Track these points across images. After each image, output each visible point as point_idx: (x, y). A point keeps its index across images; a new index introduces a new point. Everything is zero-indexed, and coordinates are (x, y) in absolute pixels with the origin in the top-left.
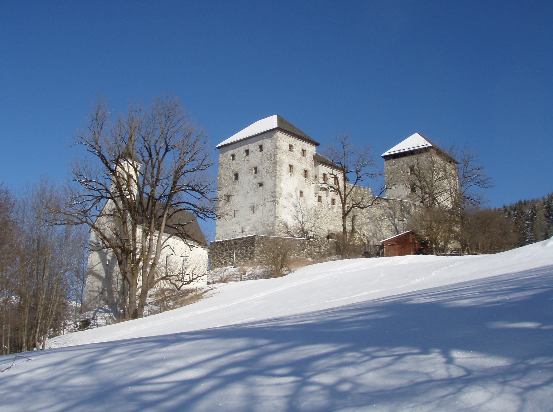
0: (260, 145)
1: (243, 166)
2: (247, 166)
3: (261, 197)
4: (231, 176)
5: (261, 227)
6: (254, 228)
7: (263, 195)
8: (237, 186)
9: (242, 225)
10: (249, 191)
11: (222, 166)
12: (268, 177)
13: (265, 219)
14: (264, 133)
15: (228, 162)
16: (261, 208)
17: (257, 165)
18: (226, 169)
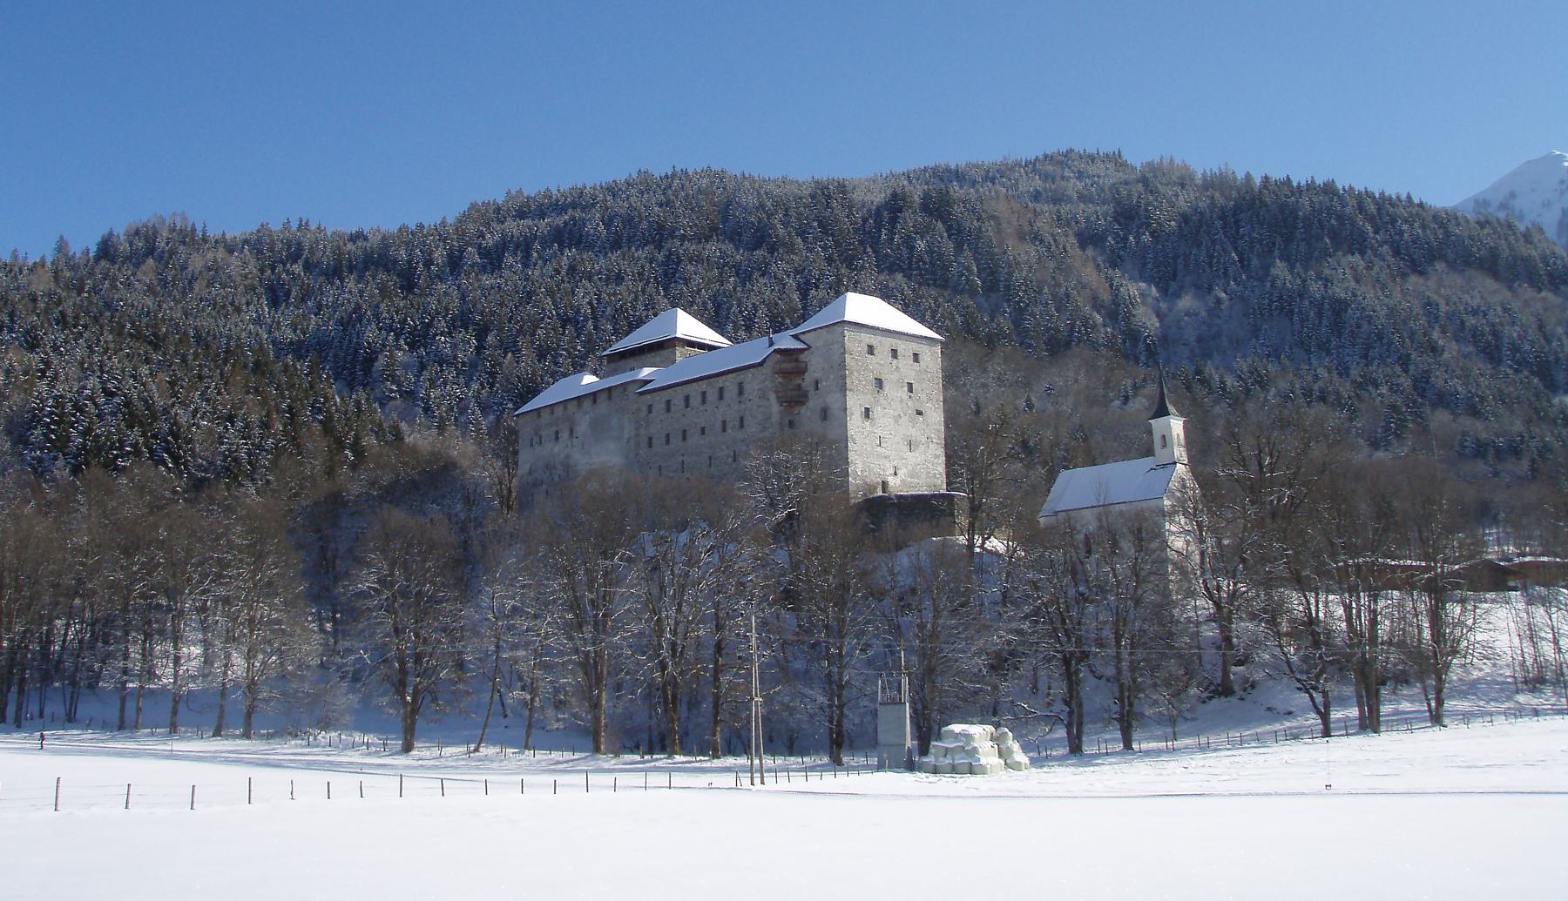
9: (895, 463)
10: (902, 415)
16: (922, 448)
17: (912, 382)
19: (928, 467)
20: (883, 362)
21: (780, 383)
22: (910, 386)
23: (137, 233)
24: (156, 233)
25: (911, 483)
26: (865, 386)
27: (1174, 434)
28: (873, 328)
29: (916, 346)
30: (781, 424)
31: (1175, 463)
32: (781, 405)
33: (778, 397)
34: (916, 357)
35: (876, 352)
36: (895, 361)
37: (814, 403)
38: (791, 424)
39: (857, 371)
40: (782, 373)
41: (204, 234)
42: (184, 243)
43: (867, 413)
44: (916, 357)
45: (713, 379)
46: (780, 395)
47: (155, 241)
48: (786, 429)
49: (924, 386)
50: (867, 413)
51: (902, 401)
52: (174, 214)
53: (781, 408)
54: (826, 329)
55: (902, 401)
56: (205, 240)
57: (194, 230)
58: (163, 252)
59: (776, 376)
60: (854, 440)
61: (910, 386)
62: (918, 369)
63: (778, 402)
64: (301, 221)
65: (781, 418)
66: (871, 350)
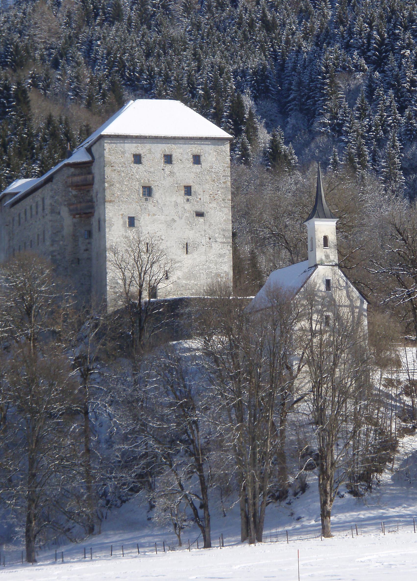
0: (195, 154)
1: (162, 178)
2: (170, 180)
3: (203, 233)
4: (137, 188)
5: (203, 276)
6: (190, 275)
7: (205, 231)
8: (150, 206)
10: (176, 218)
11: (114, 168)
12: (215, 206)
13: (212, 266)
14: (207, 139)
15: (126, 163)
16: (202, 249)
17: (191, 184)
18: (123, 175)
19: (209, 268)
21: (75, 196)
22: (188, 190)
25: (186, 284)
28: (137, 137)
29: (196, 149)
30: (74, 235)
31: (316, 266)
32: (74, 217)
33: (70, 210)
34: (197, 159)
35: (144, 160)
37: (96, 214)
39: (120, 183)
40: (76, 186)
43: (132, 222)
44: (197, 159)
45: (34, 194)
46: (72, 207)
49: (207, 186)
50: (132, 222)
51: (176, 204)
53: (75, 220)
55: (176, 204)
59: (70, 189)
61: (188, 190)
62: (198, 171)
63: (71, 215)
66: (138, 159)
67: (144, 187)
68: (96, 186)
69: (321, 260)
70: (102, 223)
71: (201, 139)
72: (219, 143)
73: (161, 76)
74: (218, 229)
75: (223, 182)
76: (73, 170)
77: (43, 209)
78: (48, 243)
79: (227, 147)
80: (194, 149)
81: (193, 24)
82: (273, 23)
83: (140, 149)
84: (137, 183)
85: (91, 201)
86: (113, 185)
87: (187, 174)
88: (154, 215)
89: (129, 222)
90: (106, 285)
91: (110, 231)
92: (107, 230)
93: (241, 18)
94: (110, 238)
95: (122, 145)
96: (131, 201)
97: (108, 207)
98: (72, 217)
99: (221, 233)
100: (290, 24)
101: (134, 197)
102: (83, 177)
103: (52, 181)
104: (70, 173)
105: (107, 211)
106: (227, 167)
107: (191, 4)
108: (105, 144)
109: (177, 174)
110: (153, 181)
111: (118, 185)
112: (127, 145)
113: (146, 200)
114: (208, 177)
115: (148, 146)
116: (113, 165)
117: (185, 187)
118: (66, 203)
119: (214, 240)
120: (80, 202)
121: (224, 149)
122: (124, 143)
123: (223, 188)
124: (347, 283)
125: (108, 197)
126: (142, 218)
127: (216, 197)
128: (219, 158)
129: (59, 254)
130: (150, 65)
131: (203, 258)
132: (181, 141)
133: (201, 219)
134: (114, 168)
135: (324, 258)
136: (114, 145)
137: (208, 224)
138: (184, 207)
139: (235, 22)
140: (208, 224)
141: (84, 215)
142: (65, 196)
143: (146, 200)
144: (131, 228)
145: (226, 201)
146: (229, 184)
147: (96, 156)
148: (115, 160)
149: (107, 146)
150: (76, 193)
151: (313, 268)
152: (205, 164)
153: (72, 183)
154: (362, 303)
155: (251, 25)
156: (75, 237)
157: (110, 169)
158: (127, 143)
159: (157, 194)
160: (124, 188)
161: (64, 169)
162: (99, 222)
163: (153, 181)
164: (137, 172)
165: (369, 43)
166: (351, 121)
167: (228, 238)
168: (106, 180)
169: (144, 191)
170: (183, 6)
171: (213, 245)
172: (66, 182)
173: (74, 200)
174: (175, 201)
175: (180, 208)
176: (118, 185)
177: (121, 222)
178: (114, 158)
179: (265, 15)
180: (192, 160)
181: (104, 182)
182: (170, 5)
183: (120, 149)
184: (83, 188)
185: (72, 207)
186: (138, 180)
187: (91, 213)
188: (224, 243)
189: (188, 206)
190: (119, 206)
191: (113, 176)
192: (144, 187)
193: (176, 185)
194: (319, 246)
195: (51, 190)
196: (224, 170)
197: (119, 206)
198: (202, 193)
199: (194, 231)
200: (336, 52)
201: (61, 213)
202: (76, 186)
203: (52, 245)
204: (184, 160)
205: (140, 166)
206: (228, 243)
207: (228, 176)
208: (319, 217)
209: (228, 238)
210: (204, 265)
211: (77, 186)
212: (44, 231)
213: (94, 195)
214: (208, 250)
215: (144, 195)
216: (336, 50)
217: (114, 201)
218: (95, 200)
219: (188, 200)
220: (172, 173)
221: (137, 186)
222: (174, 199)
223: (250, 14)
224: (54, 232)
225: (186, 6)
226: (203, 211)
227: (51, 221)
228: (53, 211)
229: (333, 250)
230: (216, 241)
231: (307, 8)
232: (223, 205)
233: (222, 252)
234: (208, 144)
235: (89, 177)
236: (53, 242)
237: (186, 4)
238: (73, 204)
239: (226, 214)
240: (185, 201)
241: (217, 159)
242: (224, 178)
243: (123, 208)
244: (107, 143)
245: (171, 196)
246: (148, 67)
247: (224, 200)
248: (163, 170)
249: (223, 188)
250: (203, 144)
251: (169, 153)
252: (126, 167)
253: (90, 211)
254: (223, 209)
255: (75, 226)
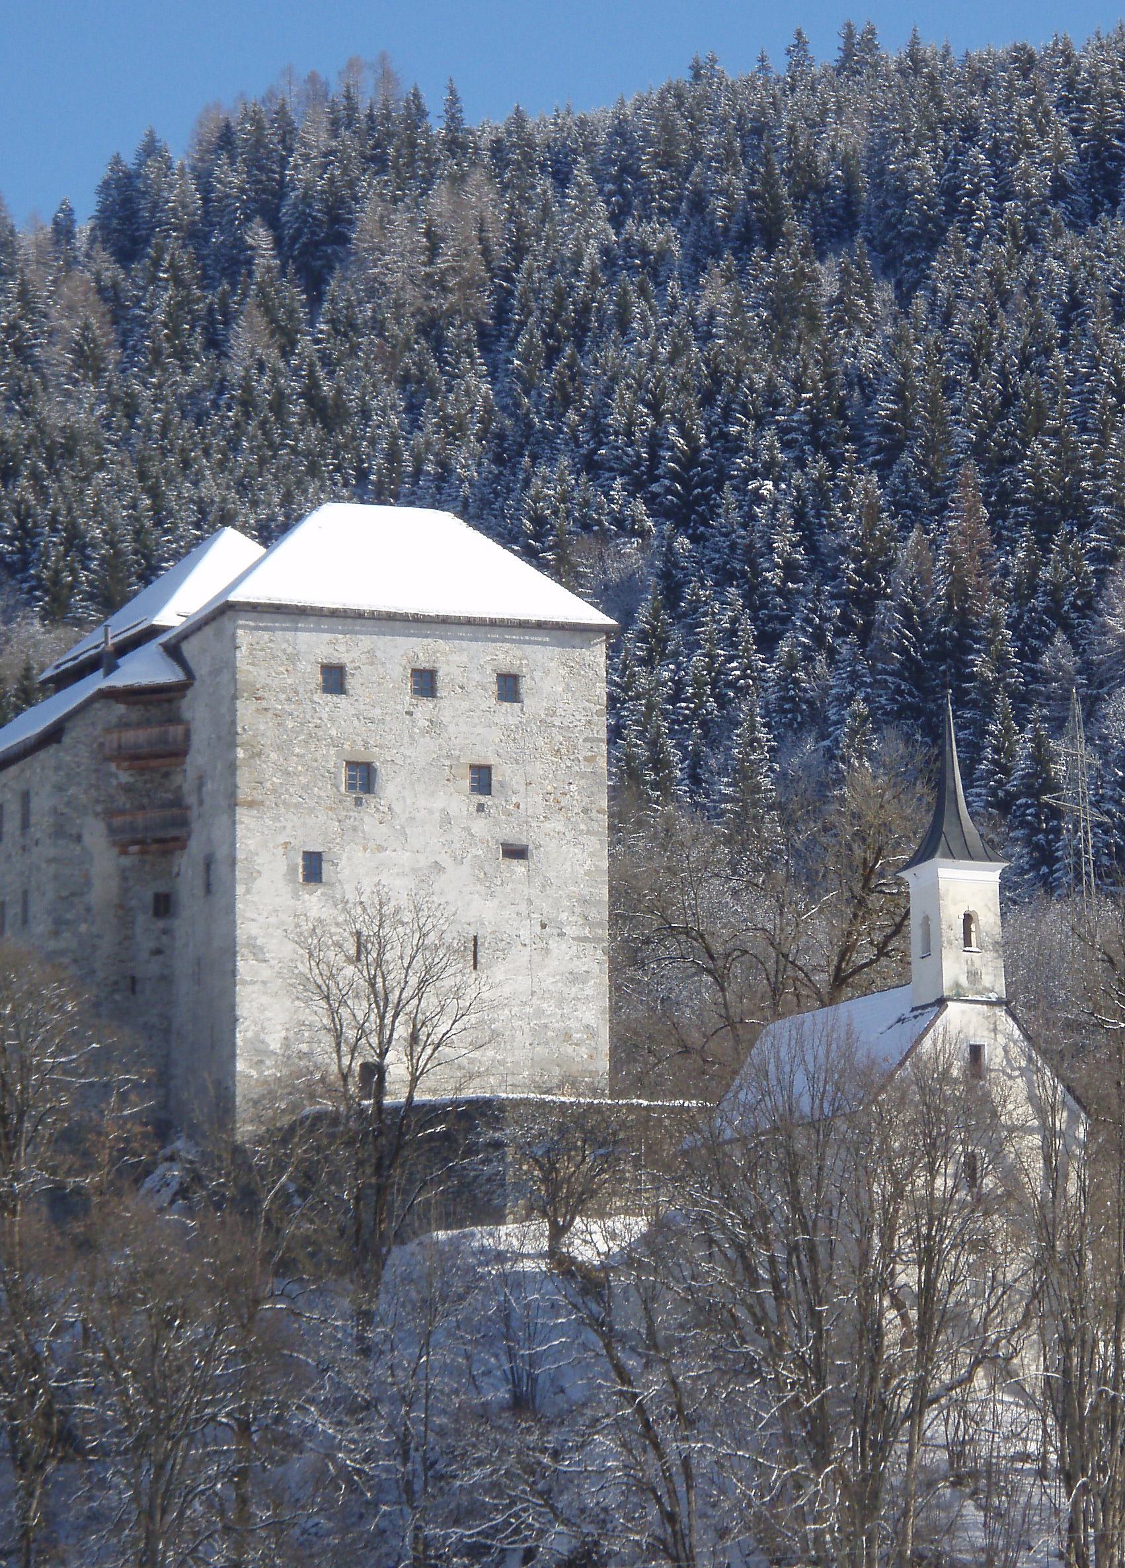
1: (406, 739)
3: (523, 907)
4: (331, 765)
5: (523, 1038)
7: (530, 902)
8: (368, 821)
10: (446, 861)
11: (264, 704)
12: (560, 827)
13: (549, 1007)
14: (540, 626)
15: (301, 690)
16: (520, 956)
17: (492, 760)
18: (290, 724)
19: (540, 1013)
20: (377, 712)
21: (128, 789)
22: (482, 779)
23: (226, 140)
24: (287, 132)
26: (306, 787)
27: (952, 915)
30: (121, 906)
31: (941, 1002)
32: (124, 852)
33: (112, 831)
35: (351, 683)
36: (425, 707)
37: (195, 846)
38: (164, 905)
39: (279, 748)
40: (134, 758)
41: (454, 120)
42: (378, 162)
46: (118, 821)
47: (284, 163)
48: (143, 919)
49: (538, 769)
51: (446, 820)
52: (353, 66)
53: (125, 861)
54: (213, 625)
55: (446, 820)
56: (455, 145)
57: (417, 113)
58: (306, 198)
59: (113, 767)
60: (258, 953)
61: (482, 779)
62: (513, 721)
63: (114, 844)
64: (849, 36)
65: (125, 891)
67: (351, 765)
68: (197, 759)
69: (958, 985)
70: (221, 869)
71: (523, 625)
72: (577, 640)
73: (54, 530)
74: (569, 897)
75: (585, 759)
76: (121, 709)
77: (25, 825)
78: (41, 926)
79: (598, 654)
80: (501, 656)
81: (114, 400)
82: (336, 405)
83: (342, 648)
84: (332, 751)
85: (178, 802)
86: (259, 755)
87: (479, 730)
88: (381, 848)
89: (305, 867)
90: (233, 1056)
91: (248, 891)
92: (240, 890)
93: (248, 389)
94: (248, 915)
95: (289, 635)
96: (312, 804)
97: (245, 819)
98: (115, 851)
99: (578, 910)
100: (383, 410)
101: (323, 794)
102: (154, 732)
103: (59, 741)
104: (114, 720)
105: (240, 831)
106: (598, 713)
107: (96, 346)
108: (240, 632)
109: (452, 728)
110: (380, 746)
111: (274, 756)
112: (303, 637)
113: (358, 802)
114: (540, 742)
115: (366, 641)
116: (260, 693)
117: (472, 767)
118: (99, 808)
119: (555, 931)
120: (142, 807)
121: (589, 658)
122: (296, 630)
123: (583, 776)
124: (1030, 1059)
125: (244, 790)
126: (345, 855)
127: (564, 801)
128: (573, 684)
129: (75, 961)
130: (23, 500)
131: (523, 983)
132: (462, 631)
133: (518, 868)
134: (264, 704)
135: (964, 981)
136: (266, 636)
137: (538, 881)
138: (467, 829)
139: (233, 397)
140: (538, 881)
141: (154, 847)
142: (97, 788)
143: (358, 802)
144: (312, 886)
145: (594, 814)
146: (603, 763)
147: (201, 669)
148: (269, 681)
149: (244, 637)
150: (131, 780)
151: (930, 1013)
152: (532, 703)
153: (120, 747)
154: (1073, 1120)
155: (279, 405)
156: (124, 912)
157: (253, 705)
158: (302, 630)
159: (390, 786)
160: (293, 765)
161: (97, 705)
162: (209, 863)
163: (380, 746)
164: (331, 719)
165: (655, 459)
166: (626, 667)
167: (599, 925)
168: (239, 740)
169: (351, 777)
170: (72, 351)
171: (553, 945)
172: (102, 745)
173: (122, 800)
174: (443, 810)
175: (456, 830)
176: (274, 756)
177: (282, 866)
178: (263, 673)
179: (314, 384)
180: (495, 687)
181: (233, 745)
182: (34, 346)
183: (284, 646)
184: (153, 763)
185: (118, 821)
186: (335, 743)
187: (175, 839)
188: (585, 939)
189: (480, 826)
190: (276, 819)
191: (262, 727)
192: (351, 765)
193: (447, 763)
194: (950, 943)
195: (57, 768)
196: (589, 722)
197: (276, 819)
198: (522, 789)
199: (496, 901)
200: (562, 480)
201: (87, 838)
202: (134, 758)
203: (56, 934)
204: (470, 687)
205: (341, 700)
206: (600, 940)
207: (601, 740)
208: (951, 854)
209: (599, 925)
210: (524, 1004)
211: (135, 757)
212: (25, 893)
213: (188, 785)
214: (537, 958)
215: (351, 787)
216: (562, 473)
217: (262, 803)
218: (191, 800)
219: (481, 808)
220: (435, 725)
221: (333, 761)
222: (439, 803)
223: (275, 379)
224: (64, 893)
225: (82, 351)
226: (524, 841)
227: (49, 861)
228: (59, 832)
229: (990, 955)
230: (561, 935)
231: (422, 372)
232: (583, 827)
233: (581, 966)
234: (544, 644)
235: (176, 731)
236: (59, 925)
237: (81, 346)
238: (122, 812)
239: (592, 855)
240: (473, 809)
241: (568, 688)
242: (588, 745)
243: (289, 825)
244: (244, 627)
245: (432, 794)
246: (19, 503)
247: (586, 811)
248: (410, 713)
249: (583, 776)
250: (529, 643)
251: (427, 666)
252: (299, 702)
253: (174, 832)
254: (584, 839)
255: (125, 879)
